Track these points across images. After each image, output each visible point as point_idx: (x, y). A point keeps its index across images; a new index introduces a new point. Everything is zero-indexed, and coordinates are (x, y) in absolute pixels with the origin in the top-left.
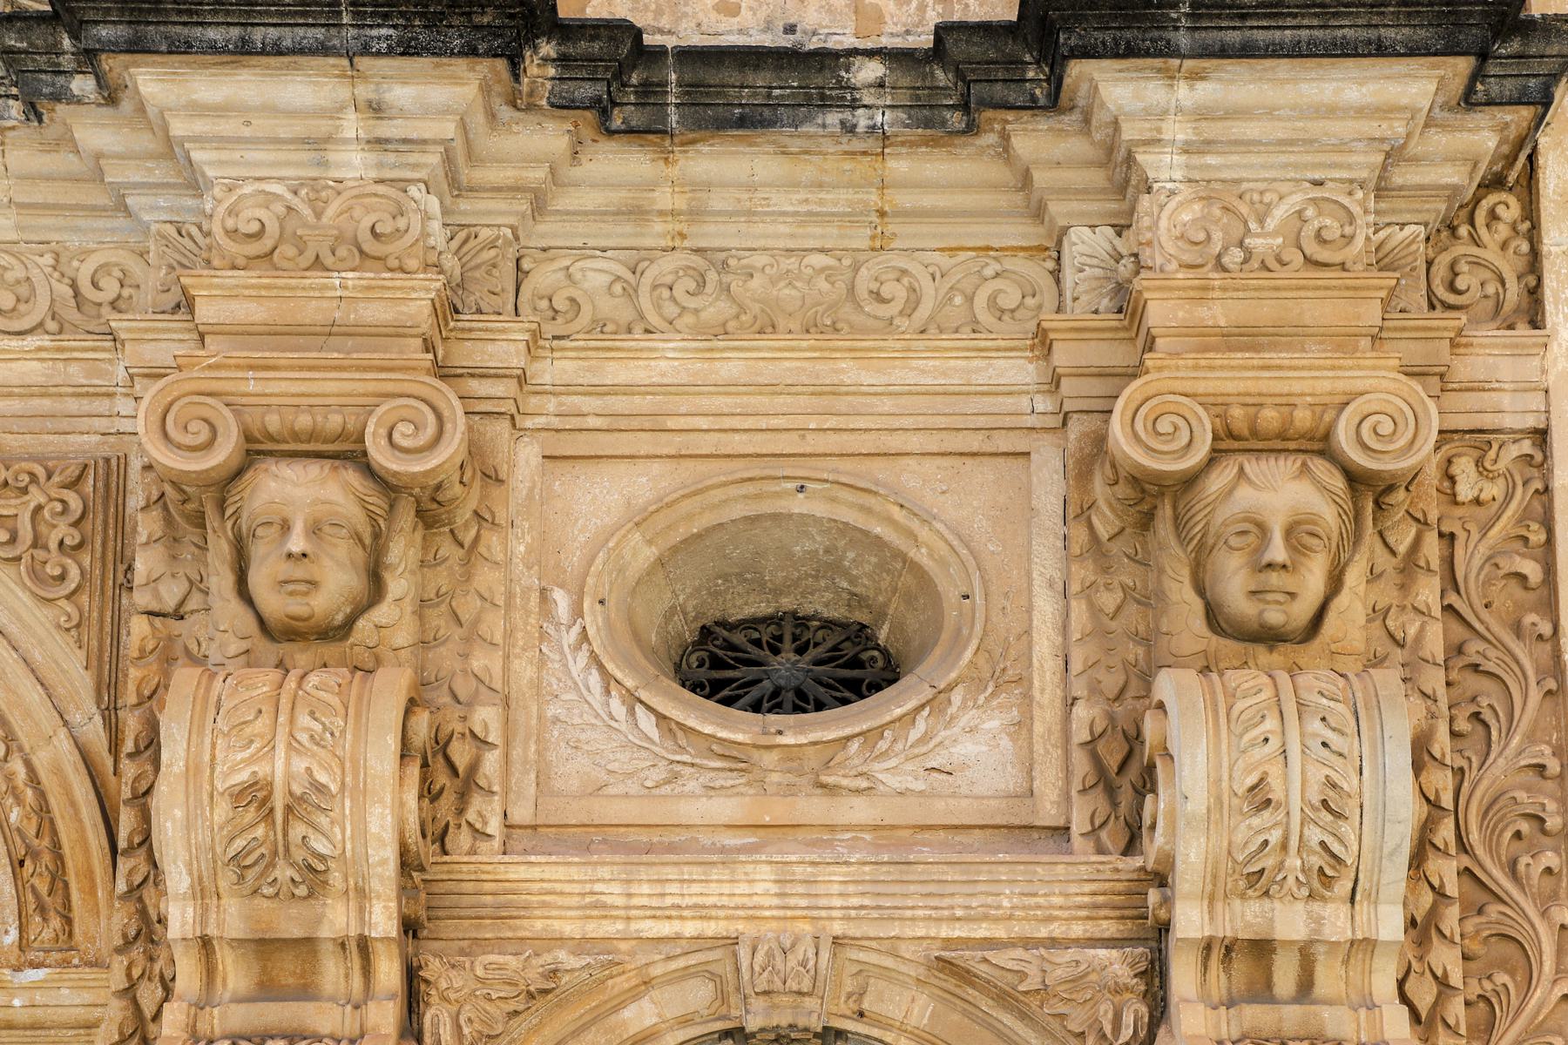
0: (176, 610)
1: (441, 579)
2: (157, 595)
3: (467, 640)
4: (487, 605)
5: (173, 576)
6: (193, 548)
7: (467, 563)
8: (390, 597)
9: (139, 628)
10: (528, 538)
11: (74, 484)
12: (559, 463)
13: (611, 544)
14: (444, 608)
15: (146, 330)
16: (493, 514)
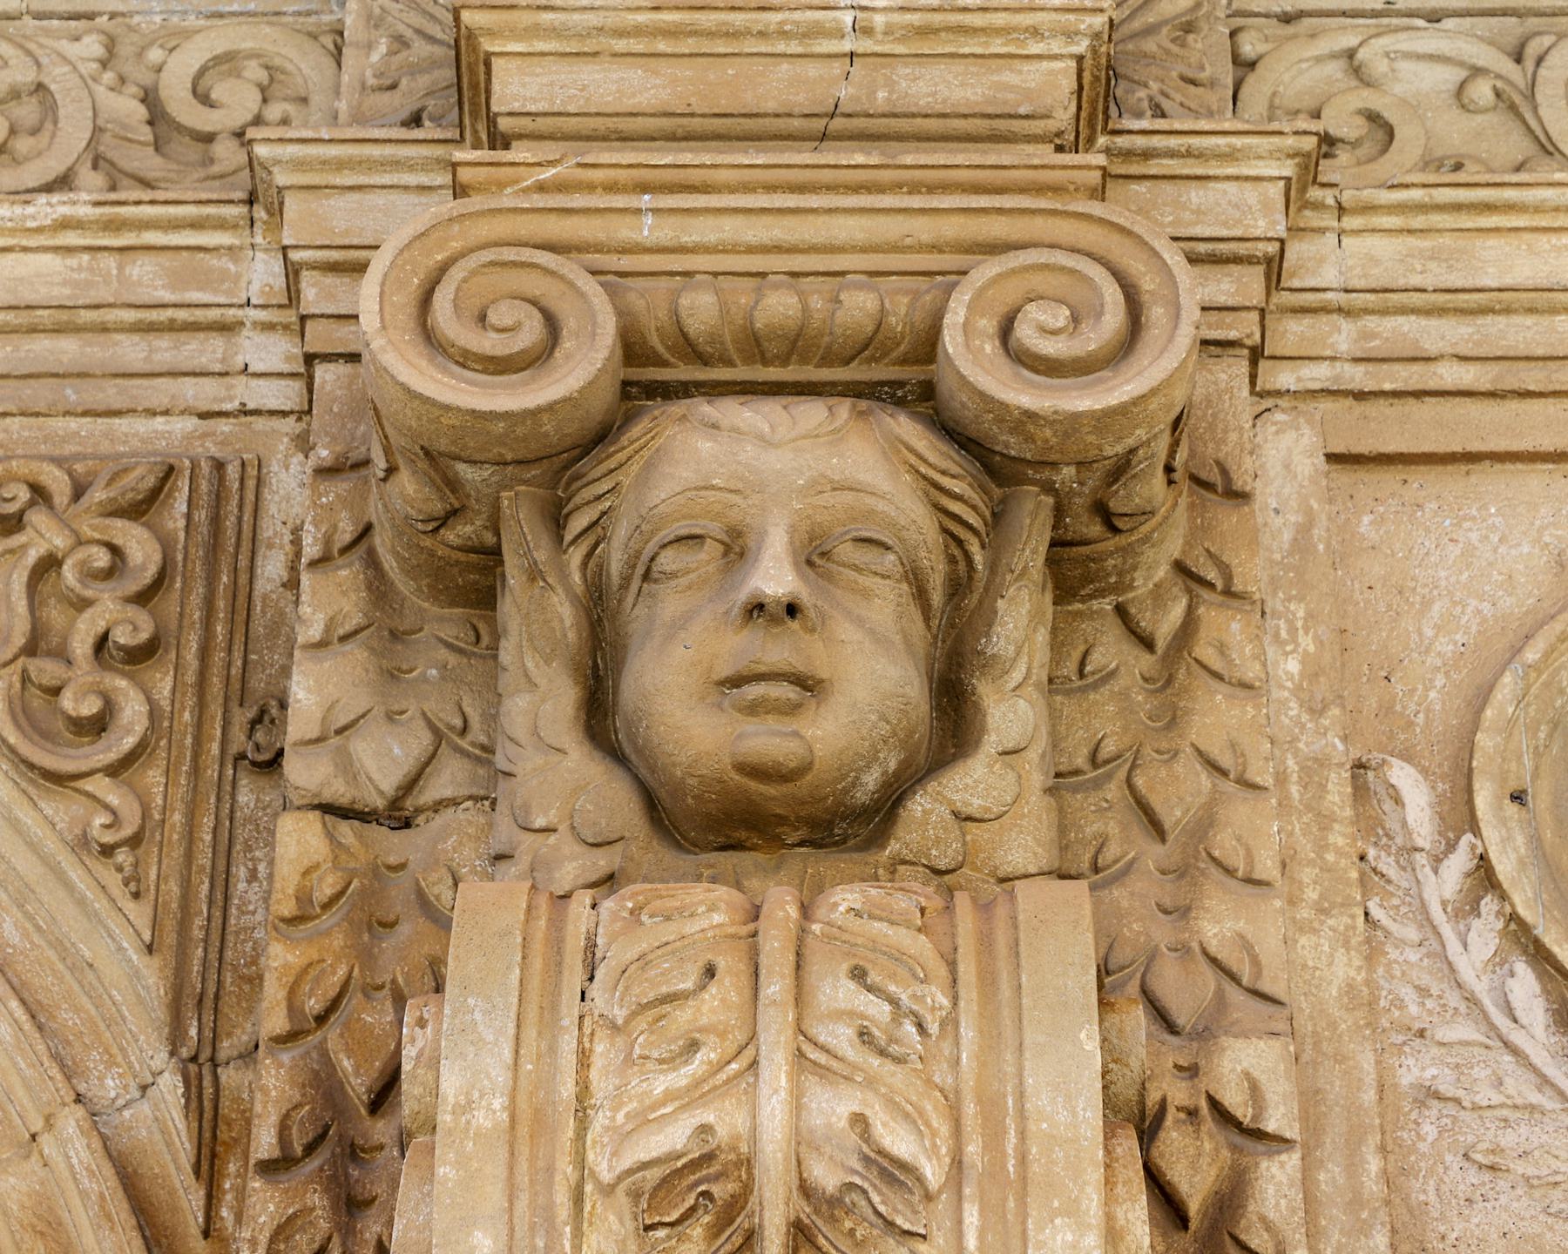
0: (395, 803)
1: (1104, 722)
2: (347, 766)
3: (1180, 872)
4: (1229, 786)
5: (391, 717)
6: (443, 653)
7: (1164, 682)
8: (991, 743)
9: (299, 843)
10: (1307, 643)
11: (140, 508)
12: (1363, 475)
13: (1531, 655)
14: (1114, 790)
15: (341, 165)
16: (1226, 571)
